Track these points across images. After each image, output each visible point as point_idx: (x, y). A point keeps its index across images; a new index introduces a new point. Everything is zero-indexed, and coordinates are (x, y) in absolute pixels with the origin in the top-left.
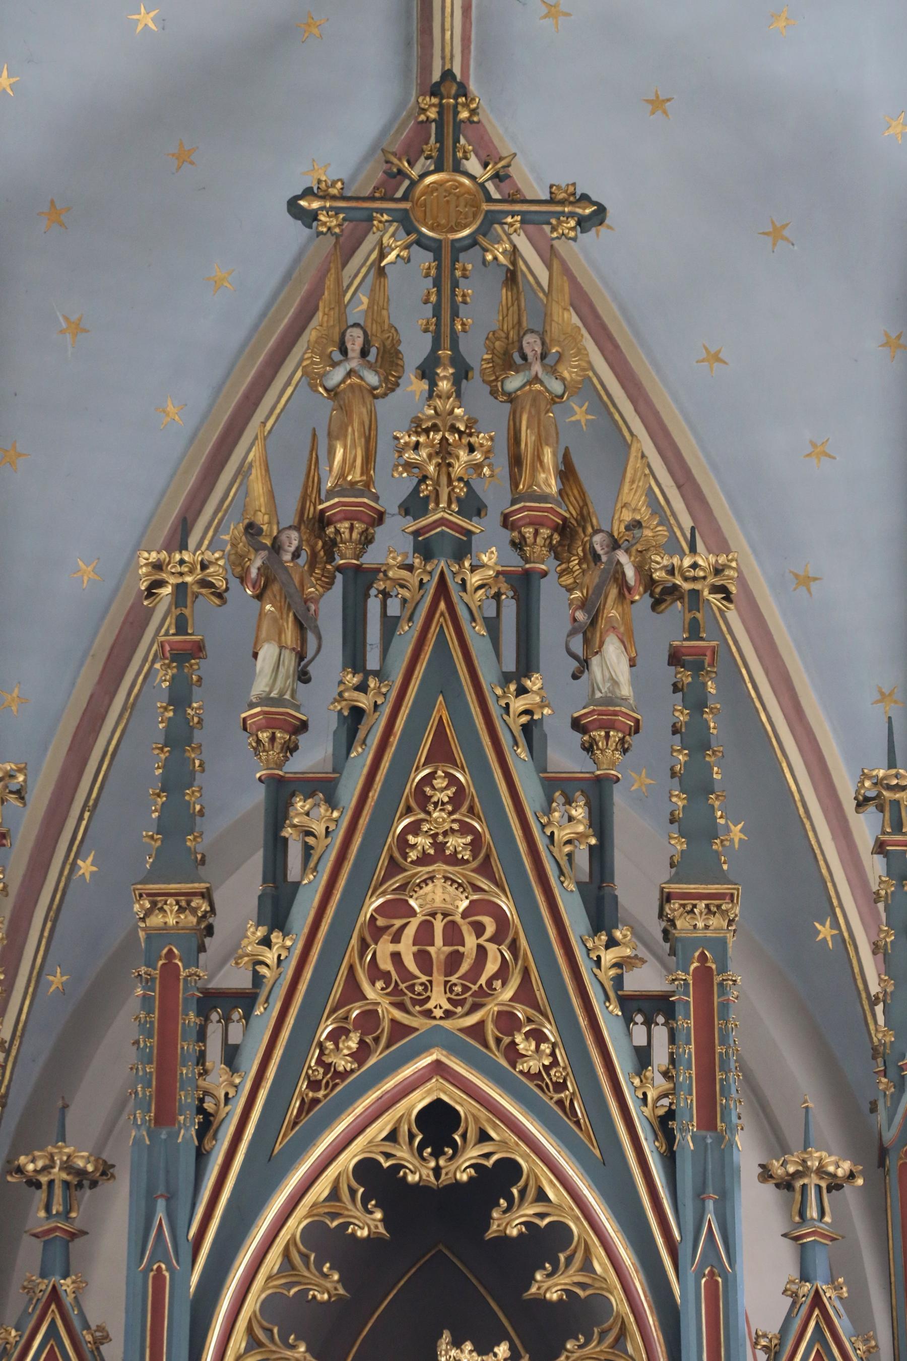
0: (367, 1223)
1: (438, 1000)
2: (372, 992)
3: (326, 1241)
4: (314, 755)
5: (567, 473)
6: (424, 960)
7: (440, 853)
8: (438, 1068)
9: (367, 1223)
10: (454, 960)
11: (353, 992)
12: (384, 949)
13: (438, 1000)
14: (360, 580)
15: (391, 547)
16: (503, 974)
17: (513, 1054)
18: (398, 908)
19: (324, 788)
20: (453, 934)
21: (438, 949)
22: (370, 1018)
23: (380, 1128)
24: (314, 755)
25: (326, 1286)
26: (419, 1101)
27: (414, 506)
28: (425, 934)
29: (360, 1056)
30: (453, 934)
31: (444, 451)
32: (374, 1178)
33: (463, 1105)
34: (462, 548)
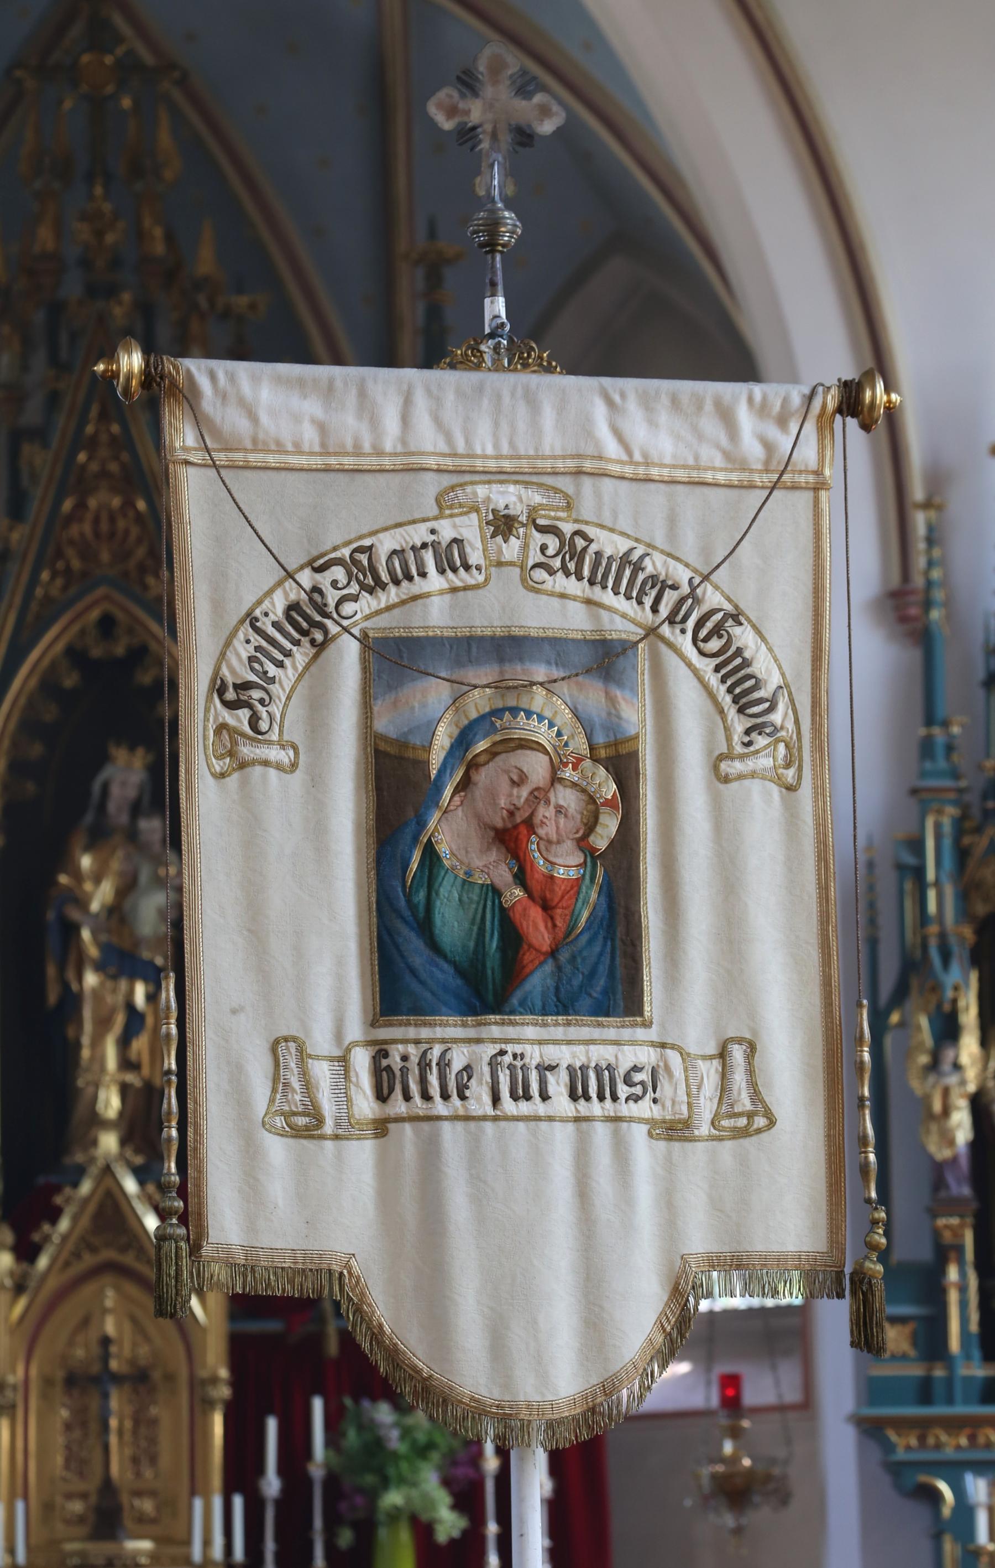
0: (70, 681)
1: (105, 556)
2: (70, 552)
3: (48, 686)
4: (32, 414)
5: (169, 238)
6: (97, 534)
7: (104, 474)
8: (107, 598)
9: (70, 681)
10: (112, 535)
11: (59, 554)
12: (74, 530)
13: (105, 556)
14: (56, 309)
15: (72, 288)
16: (139, 541)
17: (145, 587)
18: (81, 505)
19: (40, 435)
20: (112, 520)
21: (104, 527)
22: (68, 570)
23: (75, 628)
24: (32, 414)
25: (50, 713)
26: (95, 614)
27: (85, 263)
28: (96, 521)
29: (65, 588)
30: (112, 520)
31: (99, 234)
32: (75, 655)
33: (119, 615)
34: (111, 291)
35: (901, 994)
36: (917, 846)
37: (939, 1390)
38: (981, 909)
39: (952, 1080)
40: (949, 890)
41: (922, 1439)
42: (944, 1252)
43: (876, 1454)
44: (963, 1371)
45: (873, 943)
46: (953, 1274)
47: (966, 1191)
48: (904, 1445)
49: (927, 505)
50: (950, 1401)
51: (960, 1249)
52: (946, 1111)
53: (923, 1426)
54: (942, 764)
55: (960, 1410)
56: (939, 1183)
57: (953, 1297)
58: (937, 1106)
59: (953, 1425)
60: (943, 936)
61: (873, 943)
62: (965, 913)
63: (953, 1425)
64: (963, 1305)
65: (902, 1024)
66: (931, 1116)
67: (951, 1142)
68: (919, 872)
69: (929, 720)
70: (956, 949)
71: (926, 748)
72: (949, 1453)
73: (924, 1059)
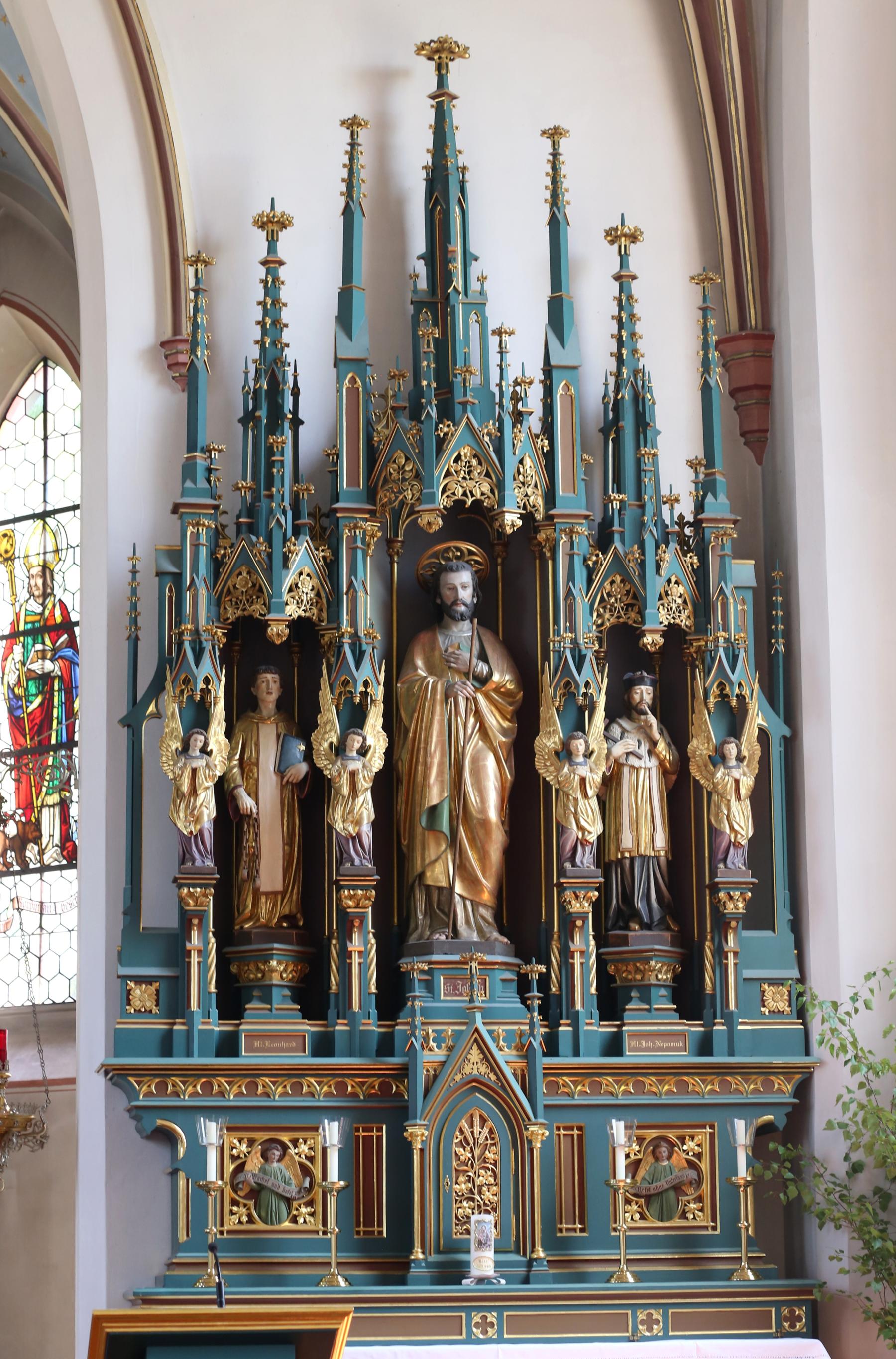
35: (157, 688)
36: (176, 555)
37: (178, 1043)
38: (232, 614)
39: (200, 763)
40: (203, 593)
41: (162, 1088)
42: (186, 920)
43: (122, 1102)
44: (199, 1026)
45: (134, 641)
46: (195, 939)
47: (210, 863)
48: (145, 1093)
49: (196, 260)
50: (189, 1054)
51: (201, 916)
52: (194, 791)
53: (163, 1073)
54: (202, 484)
55: (196, 1061)
56: (185, 856)
57: (195, 959)
58: (185, 788)
59: (189, 1073)
60: (196, 632)
61: (134, 641)
62: (219, 618)
63: (189, 1073)
64: (203, 967)
65: (158, 715)
66: (180, 795)
67: (198, 820)
68: (178, 578)
69: (192, 446)
70: (208, 646)
71: (188, 471)
72: (186, 1100)
73: (176, 745)
